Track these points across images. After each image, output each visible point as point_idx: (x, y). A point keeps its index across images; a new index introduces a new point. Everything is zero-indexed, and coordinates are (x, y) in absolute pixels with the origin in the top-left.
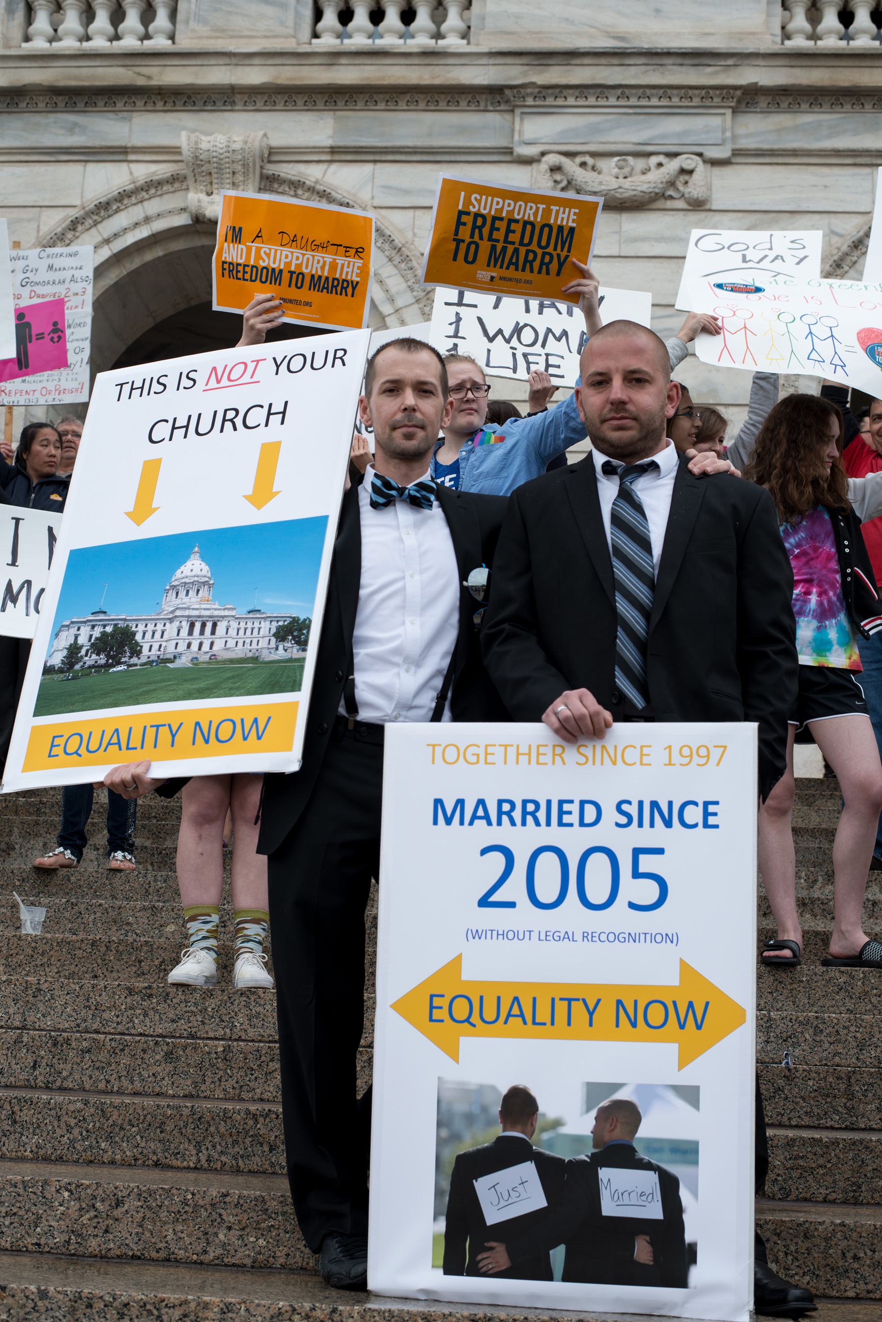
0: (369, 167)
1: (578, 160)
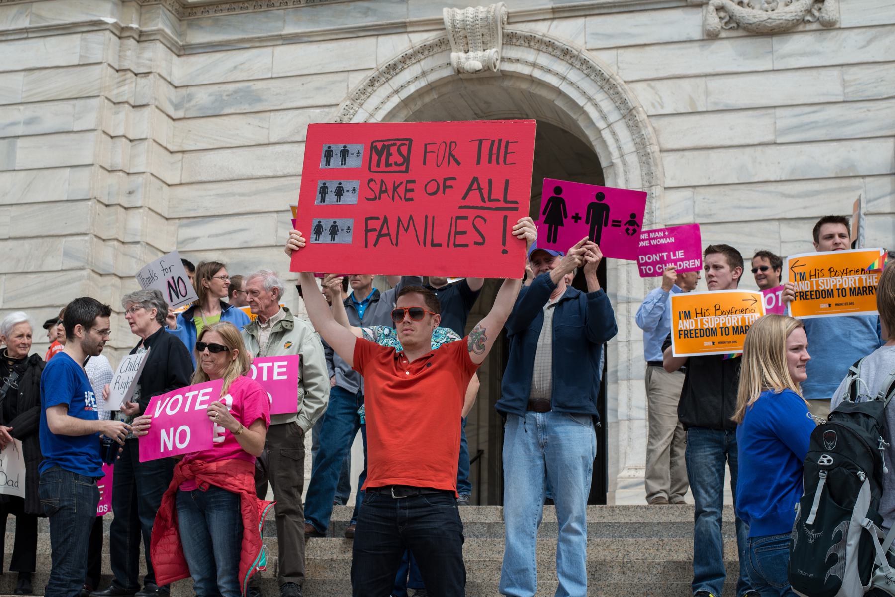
0: (580, 21)
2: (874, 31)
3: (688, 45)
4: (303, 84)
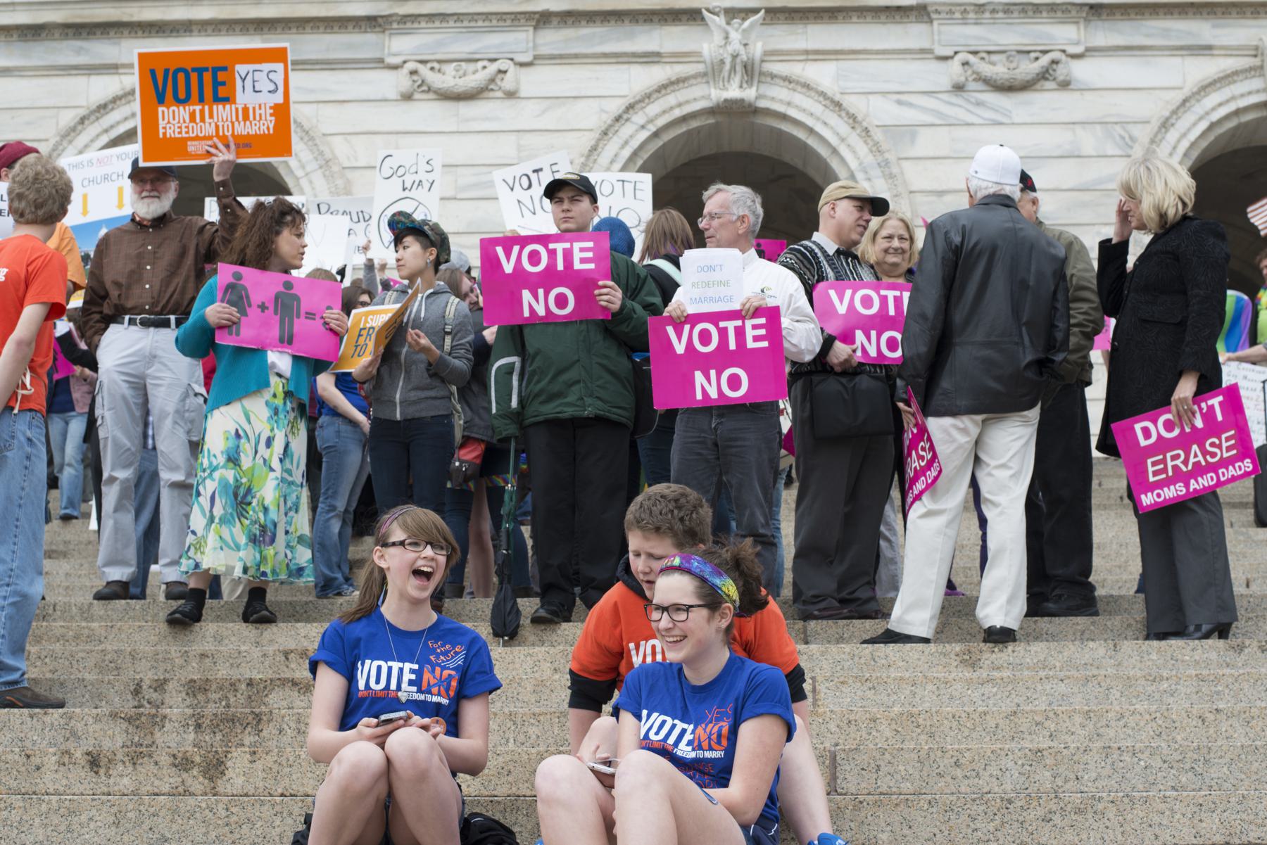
1: (429, 65)
2: (548, 102)
3: (383, 104)
4: (13, 118)
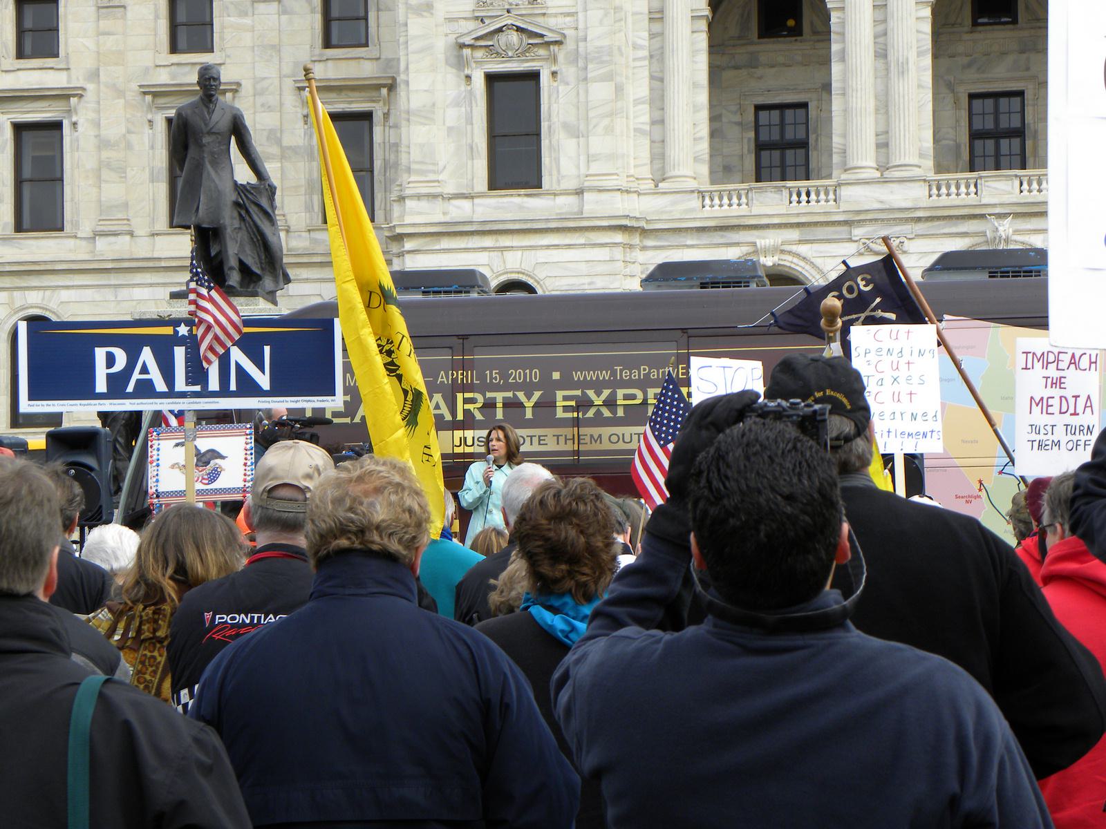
0: (810, 245)
2: (921, 255)
